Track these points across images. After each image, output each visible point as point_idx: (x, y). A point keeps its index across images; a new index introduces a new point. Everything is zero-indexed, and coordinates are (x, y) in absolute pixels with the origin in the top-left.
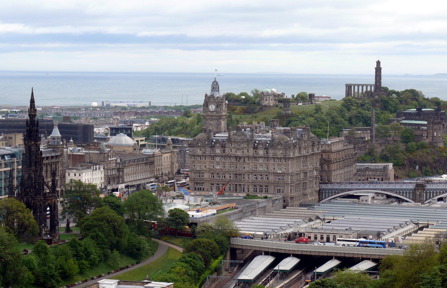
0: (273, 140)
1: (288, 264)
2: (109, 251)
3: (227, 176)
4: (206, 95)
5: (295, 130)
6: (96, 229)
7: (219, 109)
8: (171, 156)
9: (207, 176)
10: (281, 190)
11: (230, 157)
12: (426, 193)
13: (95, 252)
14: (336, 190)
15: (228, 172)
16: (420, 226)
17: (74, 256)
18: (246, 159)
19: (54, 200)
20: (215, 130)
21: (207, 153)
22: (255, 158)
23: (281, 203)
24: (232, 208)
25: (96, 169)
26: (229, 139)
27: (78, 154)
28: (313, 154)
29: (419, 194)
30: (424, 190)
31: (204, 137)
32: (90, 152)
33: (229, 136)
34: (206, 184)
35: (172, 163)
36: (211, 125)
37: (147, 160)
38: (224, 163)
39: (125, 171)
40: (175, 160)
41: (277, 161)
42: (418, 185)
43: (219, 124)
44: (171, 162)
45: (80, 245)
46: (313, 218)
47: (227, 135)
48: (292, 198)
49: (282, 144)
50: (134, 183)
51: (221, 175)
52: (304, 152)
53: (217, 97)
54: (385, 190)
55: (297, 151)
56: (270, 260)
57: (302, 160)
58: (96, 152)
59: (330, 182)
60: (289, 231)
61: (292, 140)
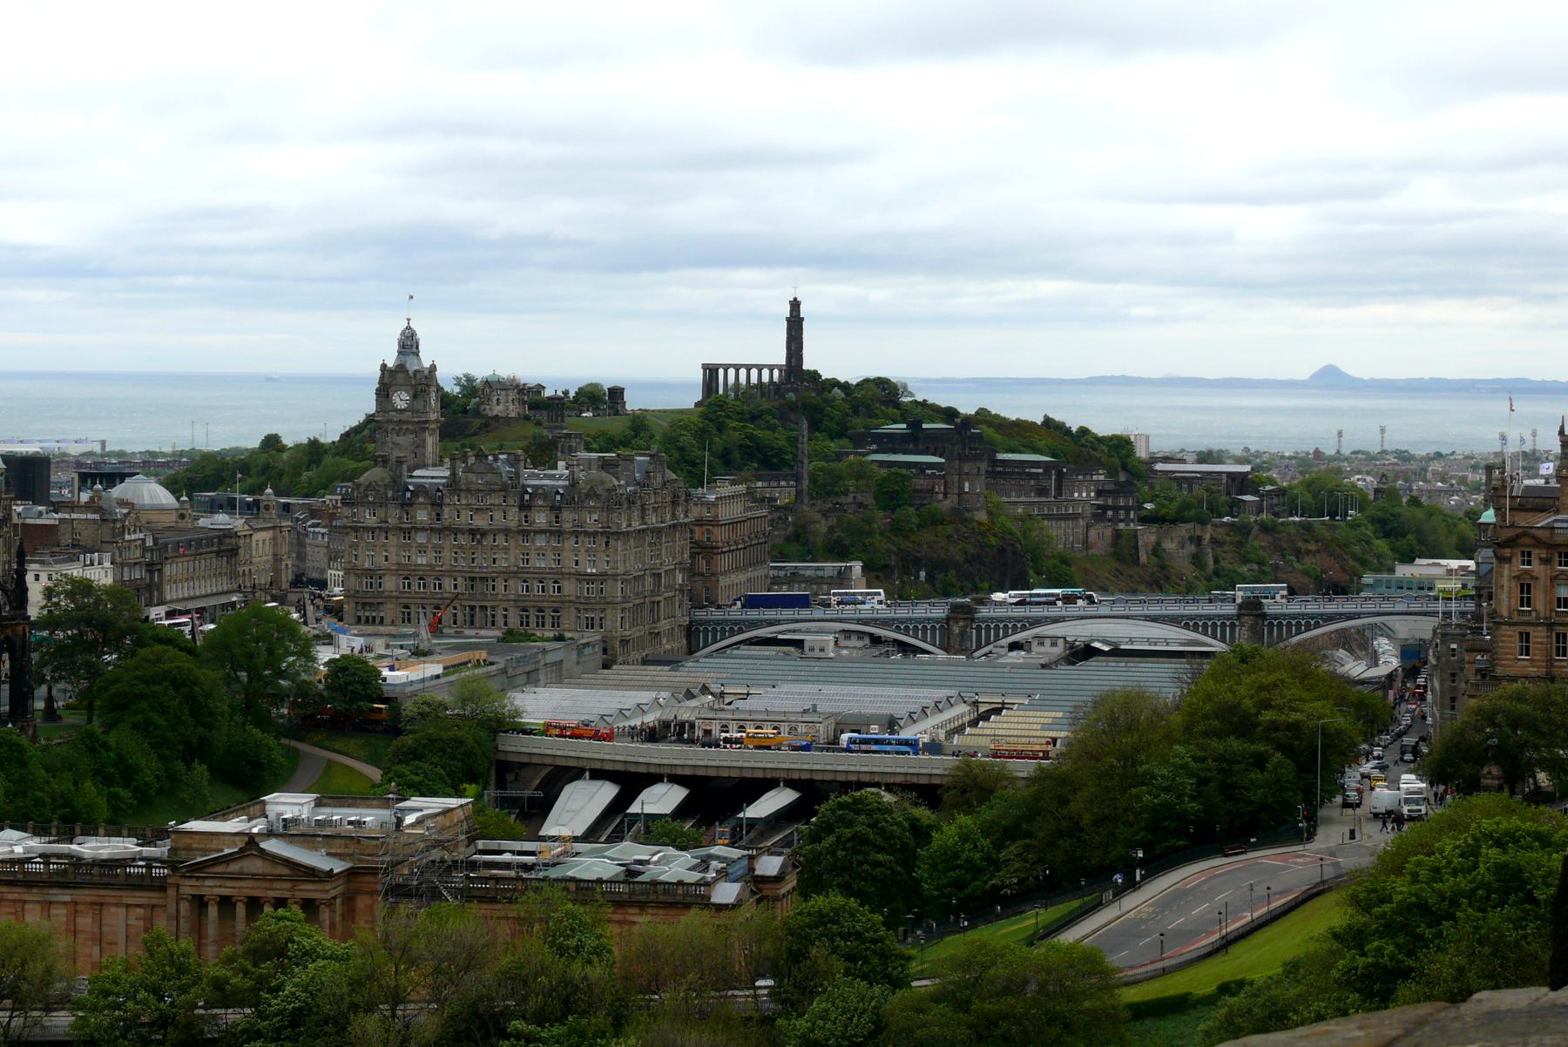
0: (574, 483)
1: (661, 800)
2: (180, 765)
3: (448, 584)
4: (384, 366)
5: (630, 459)
6: (144, 705)
7: (419, 404)
8: (274, 538)
9: (390, 584)
10: (597, 622)
11: (456, 532)
12: (979, 628)
13: (149, 767)
14: (736, 622)
15: (450, 573)
16: (983, 709)
17: (97, 773)
18: (500, 540)
19: (20, 628)
20: (411, 461)
21: (392, 521)
22: (525, 533)
23: (599, 657)
24: (478, 664)
25: (92, 564)
26: (453, 484)
27: (39, 522)
28: (674, 526)
29: (961, 634)
30: (973, 620)
31: (382, 479)
32: (74, 516)
33: (454, 474)
34: (389, 606)
35: (277, 558)
36: (398, 445)
37: (220, 543)
38: (438, 550)
39: (167, 570)
40: (285, 549)
41: (587, 542)
42: (955, 608)
43: (422, 444)
44: (275, 555)
45: (105, 746)
46: (696, 691)
47: (447, 473)
48: (624, 642)
49: (598, 496)
50: (190, 605)
51: (430, 581)
52: (652, 519)
53: (416, 372)
54: (866, 622)
55: (636, 514)
56: (607, 792)
57: (648, 539)
58: (90, 516)
59: (713, 603)
60: (651, 719)
61: (622, 484)
